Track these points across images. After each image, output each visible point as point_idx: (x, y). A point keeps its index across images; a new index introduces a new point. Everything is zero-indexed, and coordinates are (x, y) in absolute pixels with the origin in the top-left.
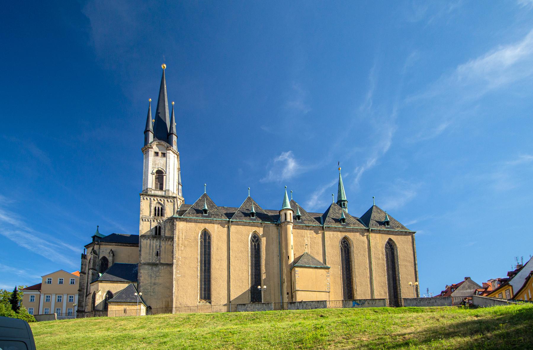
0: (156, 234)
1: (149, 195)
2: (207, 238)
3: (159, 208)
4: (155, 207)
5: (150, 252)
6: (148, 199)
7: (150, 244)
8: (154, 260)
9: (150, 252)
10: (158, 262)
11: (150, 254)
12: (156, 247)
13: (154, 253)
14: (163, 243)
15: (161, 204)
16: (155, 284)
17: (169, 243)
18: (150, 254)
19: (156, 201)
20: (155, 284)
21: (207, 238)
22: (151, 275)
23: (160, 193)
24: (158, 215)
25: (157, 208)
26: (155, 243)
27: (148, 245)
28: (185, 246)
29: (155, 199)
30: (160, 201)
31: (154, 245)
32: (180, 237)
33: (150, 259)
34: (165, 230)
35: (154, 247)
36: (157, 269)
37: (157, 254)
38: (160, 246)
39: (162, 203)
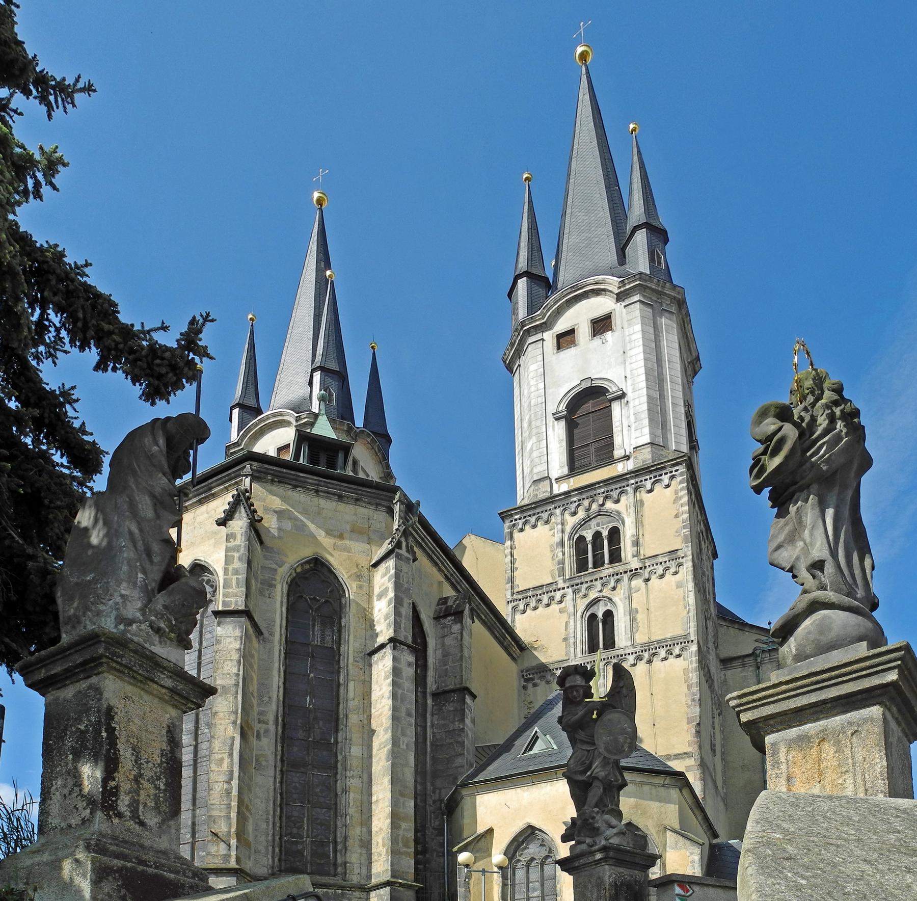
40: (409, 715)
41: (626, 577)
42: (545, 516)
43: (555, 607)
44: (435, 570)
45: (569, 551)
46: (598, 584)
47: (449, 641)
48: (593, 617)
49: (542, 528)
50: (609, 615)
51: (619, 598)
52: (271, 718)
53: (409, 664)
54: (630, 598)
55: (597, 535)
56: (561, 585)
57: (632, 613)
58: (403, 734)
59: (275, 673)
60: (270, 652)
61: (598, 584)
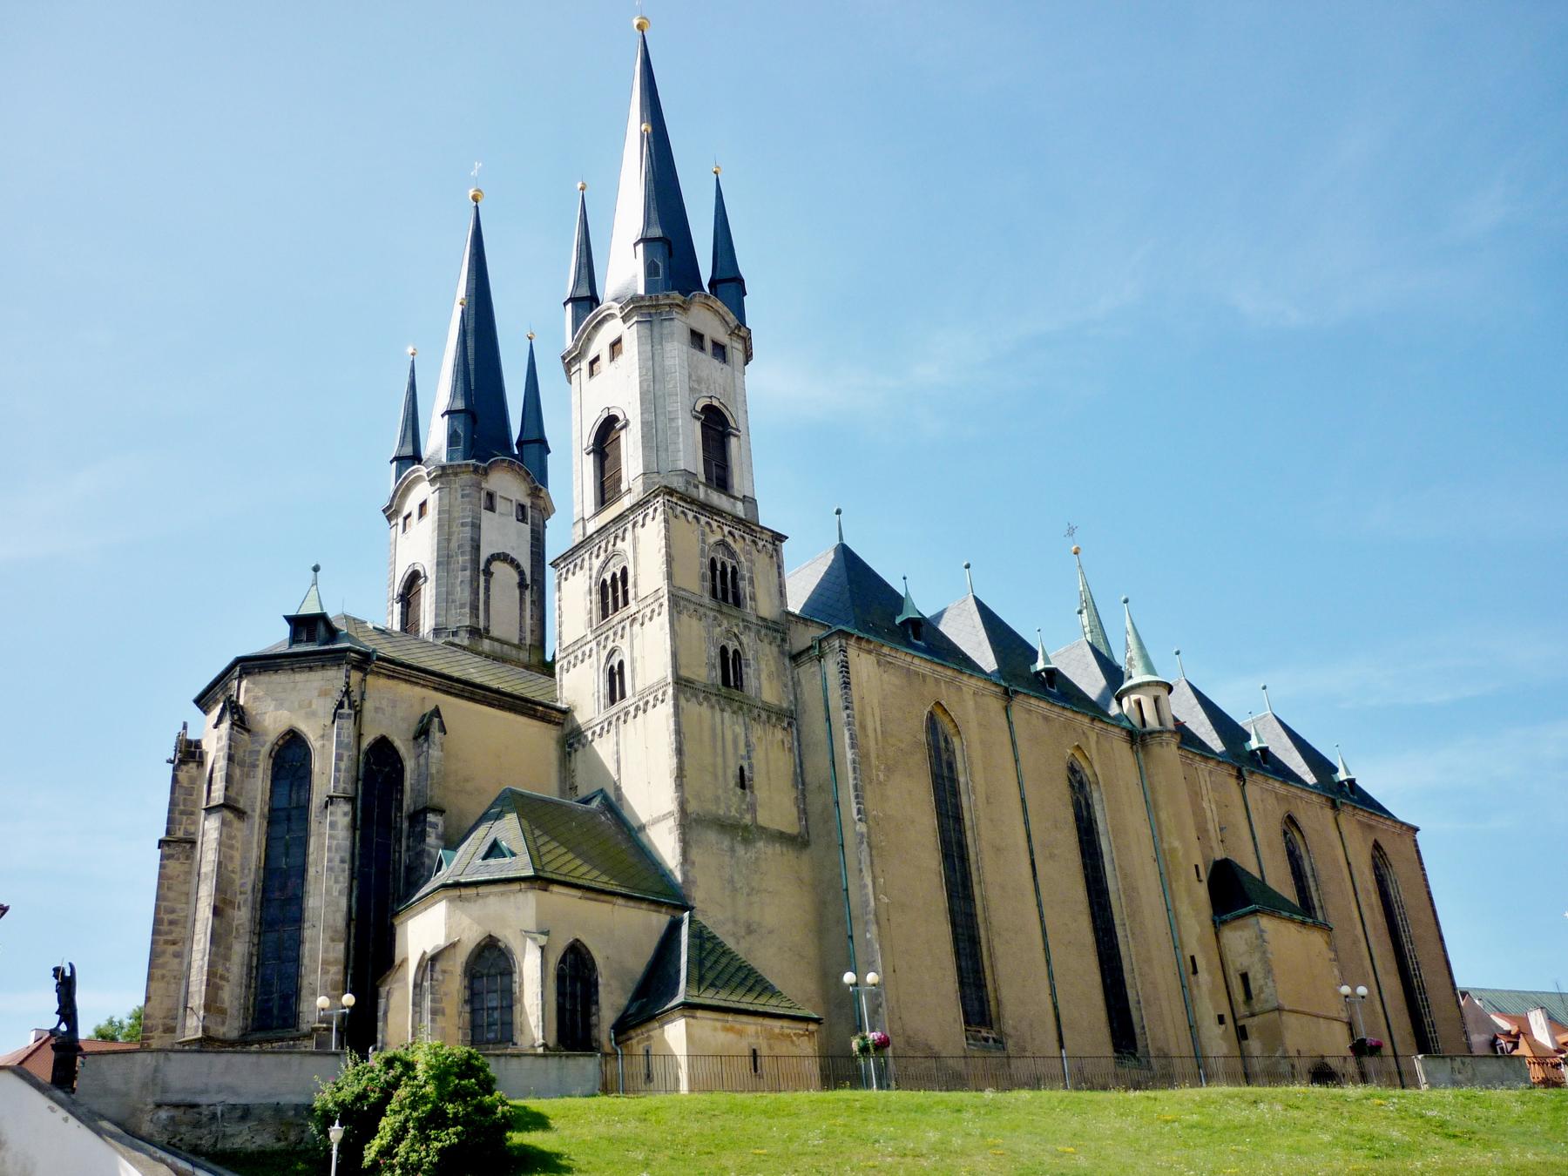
0: (726, 681)
2: (943, 744)
3: (723, 564)
4: (713, 562)
6: (690, 515)
7: (713, 729)
8: (730, 804)
9: (714, 766)
10: (748, 819)
11: (715, 776)
14: (757, 730)
15: (732, 554)
16: (750, 930)
17: (779, 734)
18: (715, 776)
19: (719, 537)
21: (943, 744)
22: (731, 881)
23: (718, 499)
24: (725, 599)
25: (719, 566)
26: (731, 726)
28: (889, 770)
29: (714, 524)
30: (729, 540)
31: (729, 736)
33: (717, 799)
34: (758, 671)
36: (752, 854)
37: (743, 782)
38: (748, 745)
39: (736, 547)
40: (342, 861)
41: (628, 622)
42: (579, 561)
43: (587, 661)
44: (418, 689)
45: (596, 597)
46: (611, 633)
47: (422, 760)
48: (612, 668)
50: (621, 664)
51: (624, 645)
52: (249, 887)
53: (345, 814)
55: (614, 575)
56: (590, 637)
57: (632, 661)
58: (336, 882)
59: (255, 845)
60: (252, 828)
61: (611, 633)
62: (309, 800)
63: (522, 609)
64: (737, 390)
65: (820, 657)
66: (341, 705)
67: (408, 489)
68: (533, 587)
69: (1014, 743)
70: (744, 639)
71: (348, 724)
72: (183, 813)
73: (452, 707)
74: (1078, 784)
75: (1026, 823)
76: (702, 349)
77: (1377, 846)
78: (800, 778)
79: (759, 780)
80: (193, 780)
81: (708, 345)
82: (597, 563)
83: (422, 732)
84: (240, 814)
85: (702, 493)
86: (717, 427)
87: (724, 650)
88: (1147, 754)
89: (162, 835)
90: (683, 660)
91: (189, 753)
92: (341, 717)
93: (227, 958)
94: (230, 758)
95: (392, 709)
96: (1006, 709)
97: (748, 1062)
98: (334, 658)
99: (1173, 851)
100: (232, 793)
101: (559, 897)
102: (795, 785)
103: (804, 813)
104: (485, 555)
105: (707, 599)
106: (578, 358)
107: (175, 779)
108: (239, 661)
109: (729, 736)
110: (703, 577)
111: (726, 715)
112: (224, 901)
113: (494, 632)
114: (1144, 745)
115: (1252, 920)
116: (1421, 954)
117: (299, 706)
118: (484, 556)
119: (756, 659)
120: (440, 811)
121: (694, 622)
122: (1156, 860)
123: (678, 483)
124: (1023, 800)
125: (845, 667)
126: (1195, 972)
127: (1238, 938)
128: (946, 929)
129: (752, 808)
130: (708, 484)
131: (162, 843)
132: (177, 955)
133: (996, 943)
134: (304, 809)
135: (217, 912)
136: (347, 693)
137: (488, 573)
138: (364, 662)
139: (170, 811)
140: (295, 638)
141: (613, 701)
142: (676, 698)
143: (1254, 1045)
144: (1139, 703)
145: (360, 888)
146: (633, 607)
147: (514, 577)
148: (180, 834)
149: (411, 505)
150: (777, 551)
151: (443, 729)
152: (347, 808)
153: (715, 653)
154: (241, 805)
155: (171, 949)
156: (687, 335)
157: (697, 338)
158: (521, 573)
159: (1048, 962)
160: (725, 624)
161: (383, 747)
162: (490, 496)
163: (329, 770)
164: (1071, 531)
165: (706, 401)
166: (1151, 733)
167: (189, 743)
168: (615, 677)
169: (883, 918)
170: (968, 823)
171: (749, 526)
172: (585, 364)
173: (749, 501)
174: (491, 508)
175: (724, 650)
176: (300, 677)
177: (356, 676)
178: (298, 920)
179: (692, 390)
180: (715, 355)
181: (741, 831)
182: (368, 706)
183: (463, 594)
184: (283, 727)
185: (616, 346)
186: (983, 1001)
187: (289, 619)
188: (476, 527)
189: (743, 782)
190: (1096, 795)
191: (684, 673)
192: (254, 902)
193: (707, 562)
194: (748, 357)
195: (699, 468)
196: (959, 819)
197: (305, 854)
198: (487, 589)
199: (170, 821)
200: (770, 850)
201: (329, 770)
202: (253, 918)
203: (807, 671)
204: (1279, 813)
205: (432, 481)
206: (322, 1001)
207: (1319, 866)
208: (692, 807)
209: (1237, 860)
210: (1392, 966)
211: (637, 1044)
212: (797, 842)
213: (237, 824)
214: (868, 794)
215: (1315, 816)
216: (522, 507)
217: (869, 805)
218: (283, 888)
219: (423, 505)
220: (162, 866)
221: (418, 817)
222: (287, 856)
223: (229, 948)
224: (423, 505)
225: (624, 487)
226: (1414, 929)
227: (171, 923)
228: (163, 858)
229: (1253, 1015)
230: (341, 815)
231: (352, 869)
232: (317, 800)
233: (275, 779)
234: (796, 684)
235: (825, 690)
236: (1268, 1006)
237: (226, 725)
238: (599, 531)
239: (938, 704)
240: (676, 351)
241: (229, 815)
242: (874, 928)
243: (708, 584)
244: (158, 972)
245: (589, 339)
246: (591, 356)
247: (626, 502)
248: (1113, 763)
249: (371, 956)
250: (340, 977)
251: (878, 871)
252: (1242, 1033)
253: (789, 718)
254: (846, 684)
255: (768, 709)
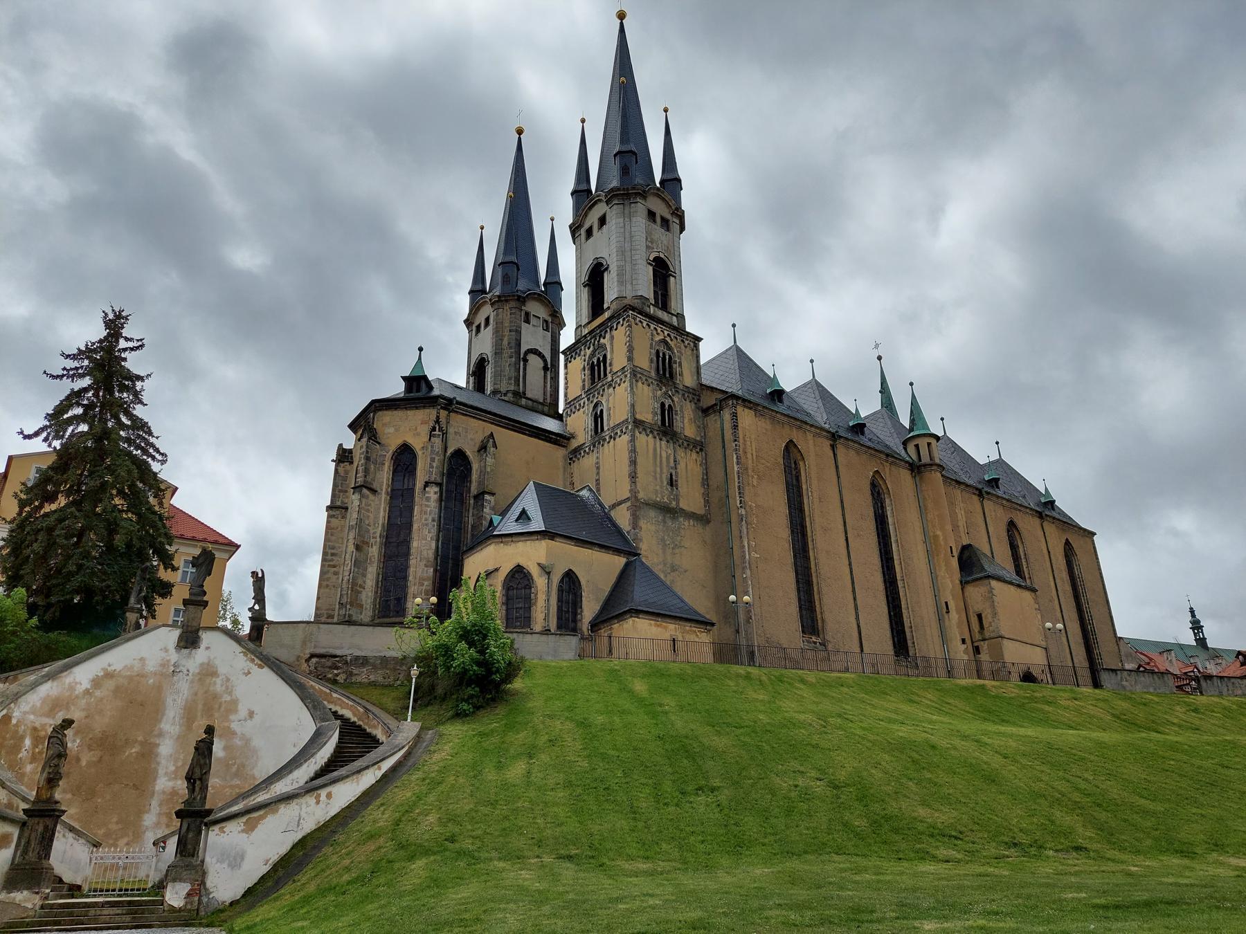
1: (641, 313)
4: (658, 352)
5: (655, 472)
7: (655, 450)
8: (664, 497)
9: (655, 472)
12: (668, 458)
13: (664, 476)
14: (681, 453)
15: (670, 348)
16: (674, 569)
17: (694, 455)
20: (674, 569)
22: (663, 540)
26: (664, 448)
27: (651, 451)
28: (759, 478)
30: (668, 339)
31: (664, 455)
32: (749, 451)
35: (664, 460)
37: (672, 482)
39: (672, 344)
49: (578, 358)
54: (608, 400)
62: (414, 485)
63: (545, 382)
64: (674, 248)
65: (722, 409)
66: (434, 429)
67: (478, 309)
68: (550, 369)
69: (837, 467)
70: (676, 399)
71: (437, 441)
72: (340, 491)
73: (502, 435)
74: (877, 493)
75: (843, 515)
76: (655, 221)
77: (1067, 543)
78: (706, 482)
79: (681, 482)
80: (347, 472)
81: (658, 219)
82: (588, 352)
83: (483, 448)
84: (374, 491)
85: (652, 310)
86: (663, 272)
87: (663, 405)
88: (921, 478)
89: (329, 503)
90: (637, 409)
91: (344, 456)
92: (434, 436)
93: (364, 575)
94: (367, 459)
95: (466, 434)
96: (833, 447)
97: (670, 643)
98: (432, 401)
99: (936, 537)
100: (369, 479)
101: (559, 546)
102: (703, 485)
103: (707, 502)
104: (524, 349)
105: (653, 374)
106: (580, 227)
107: (336, 470)
108: (373, 402)
109: (664, 455)
110: (651, 361)
111: (663, 443)
112: (363, 542)
113: (529, 395)
114: (919, 472)
115: (986, 581)
116: (1095, 612)
117: (409, 429)
118: (523, 350)
119: (682, 411)
120: (493, 494)
121: (646, 387)
122: (925, 542)
123: (636, 303)
124: (842, 502)
125: (735, 415)
126: (948, 612)
127: (976, 593)
128: (793, 575)
129: (677, 499)
130: (656, 305)
131: (329, 508)
132: (336, 573)
133: (823, 585)
134: (413, 490)
135: (358, 548)
136: (437, 421)
137: (525, 361)
138: (449, 404)
139: (333, 490)
140: (409, 389)
141: (596, 432)
142: (633, 431)
143: (984, 657)
144: (917, 446)
145: (444, 537)
146: (609, 379)
147: (541, 364)
148: (339, 503)
149: (480, 319)
150: (696, 347)
151: (495, 446)
152: (437, 489)
153: (658, 405)
154: (374, 487)
155: (333, 570)
156: (646, 213)
157: (651, 215)
158: (545, 361)
159: (855, 599)
160: (664, 389)
161: (460, 454)
162: (527, 314)
163: (427, 467)
164: (877, 346)
165: (655, 254)
166: (925, 465)
167: (345, 450)
168: (598, 418)
169: (754, 567)
170: (807, 513)
171: (680, 330)
172: (583, 231)
173: (681, 317)
174: (527, 321)
175: (663, 405)
176: (410, 413)
177: (443, 413)
178: (407, 554)
179: (648, 247)
180: (662, 226)
181: (669, 511)
182: (451, 430)
183: (508, 371)
184: (399, 442)
185: (602, 221)
186: (814, 620)
187: (404, 378)
188: (519, 332)
189: (672, 482)
190: (887, 501)
191: (638, 417)
192: (381, 544)
193: (654, 352)
194: (682, 229)
195: (651, 296)
196: (801, 510)
197: (411, 516)
198: (525, 369)
199: (333, 496)
200: (686, 523)
201: (427, 467)
202: (380, 552)
203: (712, 420)
204: (1006, 520)
205: (492, 305)
206: (418, 600)
207: (1029, 552)
208: (641, 495)
209: (975, 544)
210: (1075, 616)
211: (604, 632)
212: (703, 519)
213: (371, 497)
214: (747, 492)
215: (1028, 525)
216: (546, 321)
217: (747, 498)
218: (398, 535)
219: (487, 320)
220: (328, 522)
221: (479, 497)
222: (401, 516)
223: (366, 569)
224: (487, 320)
225: (605, 306)
226: (1090, 596)
227: (333, 554)
228: (329, 517)
229: (984, 640)
230: (433, 492)
231: (439, 526)
232: (419, 485)
233: (394, 472)
234: (705, 427)
235: (723, 430)
236: (992, 635)
237: (365, 440)
238: (590, 333)
239: (791, 441)
240: (640, 221)
241: (365, 491)
242: (748, 572)
243: (654, 365)
244: (325, 583)
245: (586, 215)
246: (587, 226)
247: (607, 315)
248: (900, 482)
249: (448, 576)
250: (430, 588)
251: (751, 537)
252: (977, 650)
253: (698, 446)
254: (735, 427)
255: (687, 439)
